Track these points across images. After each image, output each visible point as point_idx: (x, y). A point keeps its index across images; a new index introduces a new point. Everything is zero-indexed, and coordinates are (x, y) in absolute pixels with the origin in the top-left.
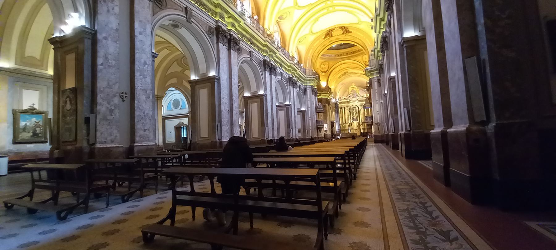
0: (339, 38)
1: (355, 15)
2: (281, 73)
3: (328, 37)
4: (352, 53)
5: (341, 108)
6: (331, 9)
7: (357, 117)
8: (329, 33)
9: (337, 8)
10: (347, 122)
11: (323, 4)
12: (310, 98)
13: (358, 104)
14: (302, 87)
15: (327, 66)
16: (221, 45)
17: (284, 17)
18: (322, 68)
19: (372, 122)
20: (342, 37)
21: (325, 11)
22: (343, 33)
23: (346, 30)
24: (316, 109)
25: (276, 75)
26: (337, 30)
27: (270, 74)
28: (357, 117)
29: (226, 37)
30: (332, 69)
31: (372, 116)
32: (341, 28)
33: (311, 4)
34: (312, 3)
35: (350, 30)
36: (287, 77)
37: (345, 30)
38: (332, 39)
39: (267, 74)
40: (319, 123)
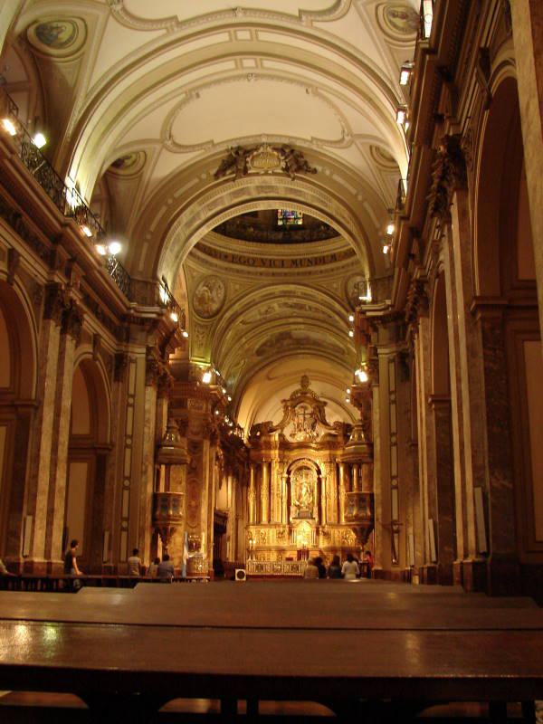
0: (266, 190)
1: (334, 106)
2: (12, 252)
3: (229, 175)
6: (249, 63)
8: (236, 161)
11: (222, 37)
15: (218, 295)
17: (64, 36)
18: (202, 300)
19: (372, 519)
20: (282, 185)
21: (229, 65)
22: (286, 169)
23: (297, 162)
26: (266, 154)
30: (237, 307)
31: (372, 495)
33: (180, 24)
34: (181, 19)
35: (313, 165)
36: (42, 281)
37: (296, 160)
38: (244, 182)
40: (166, 508)
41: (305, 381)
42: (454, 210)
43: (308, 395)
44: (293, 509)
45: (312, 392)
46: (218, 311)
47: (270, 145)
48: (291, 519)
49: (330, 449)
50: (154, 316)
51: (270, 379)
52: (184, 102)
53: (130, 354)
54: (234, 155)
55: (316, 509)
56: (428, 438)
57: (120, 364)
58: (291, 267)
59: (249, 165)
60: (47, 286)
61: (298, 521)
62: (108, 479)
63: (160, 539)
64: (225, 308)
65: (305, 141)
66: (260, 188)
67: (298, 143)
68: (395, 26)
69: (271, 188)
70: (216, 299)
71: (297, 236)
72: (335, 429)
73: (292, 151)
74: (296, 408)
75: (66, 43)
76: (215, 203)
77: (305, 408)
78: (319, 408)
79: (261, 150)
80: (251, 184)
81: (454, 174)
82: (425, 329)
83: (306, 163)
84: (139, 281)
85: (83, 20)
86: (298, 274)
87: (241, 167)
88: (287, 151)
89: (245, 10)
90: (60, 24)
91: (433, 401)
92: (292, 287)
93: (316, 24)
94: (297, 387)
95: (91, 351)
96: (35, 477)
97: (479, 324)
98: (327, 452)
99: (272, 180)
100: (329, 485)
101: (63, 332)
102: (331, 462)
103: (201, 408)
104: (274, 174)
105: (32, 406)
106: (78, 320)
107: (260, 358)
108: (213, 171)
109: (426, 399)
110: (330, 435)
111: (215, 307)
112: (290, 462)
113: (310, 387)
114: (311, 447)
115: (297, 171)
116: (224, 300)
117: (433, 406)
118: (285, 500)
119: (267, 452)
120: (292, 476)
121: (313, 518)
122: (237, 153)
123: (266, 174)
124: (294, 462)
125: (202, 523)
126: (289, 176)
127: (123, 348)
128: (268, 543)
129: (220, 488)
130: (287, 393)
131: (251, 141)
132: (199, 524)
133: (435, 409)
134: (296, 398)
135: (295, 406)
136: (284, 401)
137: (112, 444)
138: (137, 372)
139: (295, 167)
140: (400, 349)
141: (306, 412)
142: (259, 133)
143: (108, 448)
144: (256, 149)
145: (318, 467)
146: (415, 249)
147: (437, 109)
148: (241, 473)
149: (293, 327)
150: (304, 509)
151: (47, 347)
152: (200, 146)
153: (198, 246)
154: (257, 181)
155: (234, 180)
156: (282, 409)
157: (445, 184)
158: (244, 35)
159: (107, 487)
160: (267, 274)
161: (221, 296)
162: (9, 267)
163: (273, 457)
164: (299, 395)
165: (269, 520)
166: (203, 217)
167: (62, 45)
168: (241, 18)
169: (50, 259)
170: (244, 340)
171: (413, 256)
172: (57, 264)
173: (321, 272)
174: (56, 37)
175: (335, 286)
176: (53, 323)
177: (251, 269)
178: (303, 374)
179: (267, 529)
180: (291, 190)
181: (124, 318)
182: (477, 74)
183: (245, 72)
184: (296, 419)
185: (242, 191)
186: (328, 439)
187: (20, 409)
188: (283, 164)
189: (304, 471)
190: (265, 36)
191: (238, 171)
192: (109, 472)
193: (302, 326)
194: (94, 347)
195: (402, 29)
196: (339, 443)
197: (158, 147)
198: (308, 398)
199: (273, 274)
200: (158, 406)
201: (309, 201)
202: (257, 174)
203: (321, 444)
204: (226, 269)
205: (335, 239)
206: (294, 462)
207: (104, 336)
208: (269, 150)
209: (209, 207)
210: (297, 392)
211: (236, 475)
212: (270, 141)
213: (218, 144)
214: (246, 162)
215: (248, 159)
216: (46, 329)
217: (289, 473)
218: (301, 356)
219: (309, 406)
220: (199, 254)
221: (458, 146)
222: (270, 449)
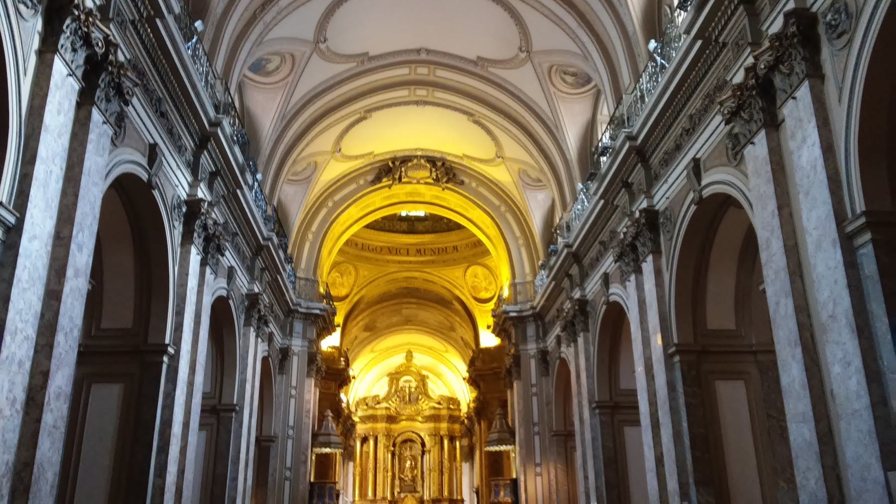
2: (231, 269)
3: (385, 181)
4: (433, 252)
5: (365, 440)
6: (422, 92)
7: (414, 479)
9: (441, 95)
10: (379, 494)
12: (300, 387)
13: (423, 429)
14: (278, 339)
16: (59, 67)
17: (271, 67)
20: (431, 192)
21: (402, 93)
24: (315, 436)
25: (215, 273)
26: (419, 167)
27: (204, 263)
28: (414, 479)
29: (87, 41)
31: (515, 482)
32: (432, 161)
34: (372, 53)
36: (244, 291)
39: (195, 257)
41: (409, 355)
42: (648, 267)
44: (397, 482)
46: (347, 296)
47: (422, 157)
48: (396, 494)
50: (318, 312)
51: (372, 351)
52: (358, 121)
53: (293, 348)
54: (390, 164)
55: (419, 482)
56: (594, 439)
57: (285, 354)
58: (415, 256)
59: (403, 174)
60: (247, 295)
61: (402, 495)
62: (271, 471)
64: (354, 292)
65: (456, 156)
66: (410, 194)
67: (449, 158)
68: (565, 81)
69: (419, 194)
70: (346, 284)
71: (420, 226)
72: (439, 403)
73: (443, 164)
75: (272, 72)
76: (367, 206)
79: (415, 161)
80: (400, 191)
81: (650, 239)
82: (586, 341)
83: (454, 175)
84: (300, 279)
85: (293, 56)
86: (422, 262)
87: (397, 177)
88: (439, 164)
89: (428, 51)
90: (270, 57)
91: (597, 407)
92: (416, 274)
93: (490, 69)
95: (267, 348)
96: (235, 479)
97: (678, 366)
98: (431, 425)
99: (422, 188)
101: (257, 336)
102: (435, 435)
103: (330, 388)
104: (427, 183)
105: (234, 410)
106: (266, 324)
108: (370, 178)
109: (590, 403)
110: (435, 408)
111: (343, 292)
112: (396, 435)
114: (416, 420)
115: (447, 182)
117: (597, 411)
118: (390, 474)
120: (397, 448)
121: (416, 491)
122: (393, 163)
123: (418, 183)
124: (399, 435)
126: (440, 186)
127: (287, 342)
131: (407, 153)
133: (600, 414)
137: (276, 437)
138: (296, 364)
139: (445, 180)
140: (541, 346)
142: (416, 147)
143: (271, 440)
144: (410, 160)
146: (575, 270)
147: (628, 177)
149: (405, 306)
150: (409, 482)
151: (247, 352)
152: (362, 156)
153: (347, 243)
154: (408, 188)
155: (390, 187)
157: (638, 244)
158: (423, 70)
159: (270, 479)
160: (394, 262)
161: (352, 280)
162: (228, 284)
165: (375, 494)
166: (356, 218)
167: (268, 74)
168: (423, 56)
169: (250, 270)
171: (570, 276)
172: (257, 273)
173: (444, 261)
174: (264, 66)
175: (457, 274)
176: (252, 329)
177: (379, 257)
178: (408, 347)
180: (437, 197)
181: (290, 313)
182: (688, 174)
183: (416, 99)
185: (393, 196)
187: (222, 414)
188: (434, 175)
189: (409, 444)
190: (443, 74)
191: (394, 179)
192: (272, 462)
193: (414, 306)
194: (269, 346)
195: (571, 85)
197: (328, 157)
198: (412, 371)
199: (399, 262)
200: (315, 394)
201: (452, 207)
202: (410, 183)
204: (357, 256)
205: (457, 232)
206: (399, 435)
207: (278, 337)
208: (422, 161)
209: (362, 209)
212: (424, 154)
213: (378, 155)
214: (401, 172)
215: (403, 169)
216: (246, 337)
217: (394, 445)
220: (347, 249)
221: (657, 219)
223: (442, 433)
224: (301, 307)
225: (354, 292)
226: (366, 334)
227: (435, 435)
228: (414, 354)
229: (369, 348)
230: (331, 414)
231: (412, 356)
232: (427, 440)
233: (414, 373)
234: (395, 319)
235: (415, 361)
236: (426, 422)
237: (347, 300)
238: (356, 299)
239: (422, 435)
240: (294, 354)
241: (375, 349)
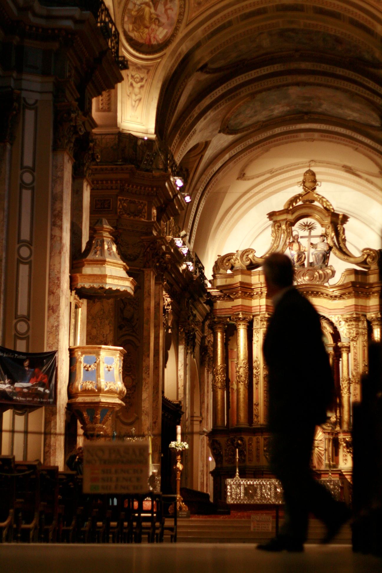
41: (311, 181)
43: (316, 203)
45: (322, 199)
49: (357, 296)
50: (69, 24)
53: (24, 94)
63: (79, 425)
64: (180, 35)
70: (164, 20)
74: (293, 228)
77: (310, 227)
78: (337, 221)
94: (299, 190)
98: (351, 302)
100: (355, 360)
102: (357, 320)
107: (230, 138)
110: (356, 272)
111: (161, 34)
113: (318, 190)
116: (179, 22)
119: (247, 302)
125: (143, 417)
128: (250, 460)
129: (165, 366)
130: (279, 201)
132: (138, 419)
134: (295, 209)
135: (292, 224)
136: (271, 215)
141: (313, 233)
145: (335, 329)
148: (198, 341)
156: (270, 230)
161: (174, 13)
163: (255, 311)
164: (300, 203)
170: (207, 101)
179: (246, 438)
184: (295, 246)
186: (352, 278)
196: (371, 285)
203: (342, 287)
210: (295, 199)
211: (190, 344)
218: (302, 135)
219: (318, 225)
222: (251, 296)
223: (371, 315)
224: (35, 15)
225: (180, 35)
226: (226, 139)
227: (357, 320)
228: (318, 177)
229: (235, 169)
230: (107, 227)
231: (315, 181)
232: (344, 330)
233: (320, 211)
234: (278, 110)
235: (320, 190)
236: (341, 297)
237: (168, 51)
238: (185, 48)
239: (334, 319)
240: (27, 106)
241: (249, 173)
